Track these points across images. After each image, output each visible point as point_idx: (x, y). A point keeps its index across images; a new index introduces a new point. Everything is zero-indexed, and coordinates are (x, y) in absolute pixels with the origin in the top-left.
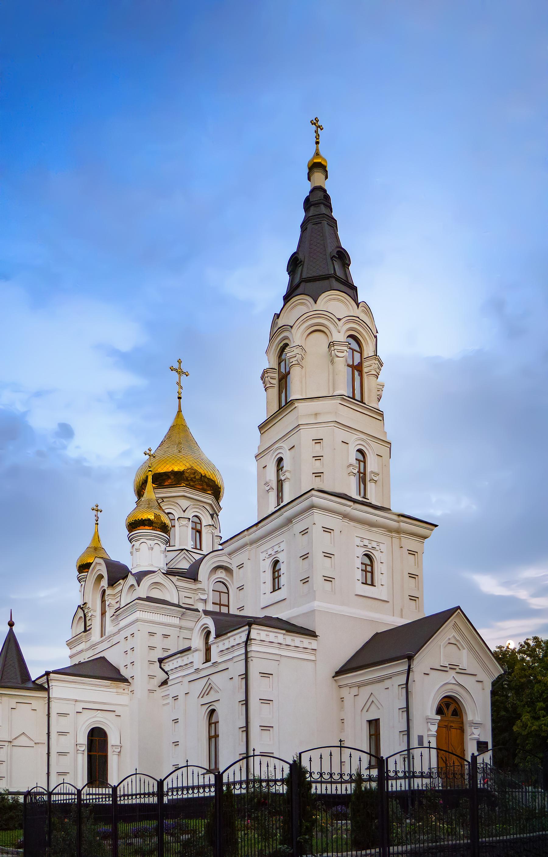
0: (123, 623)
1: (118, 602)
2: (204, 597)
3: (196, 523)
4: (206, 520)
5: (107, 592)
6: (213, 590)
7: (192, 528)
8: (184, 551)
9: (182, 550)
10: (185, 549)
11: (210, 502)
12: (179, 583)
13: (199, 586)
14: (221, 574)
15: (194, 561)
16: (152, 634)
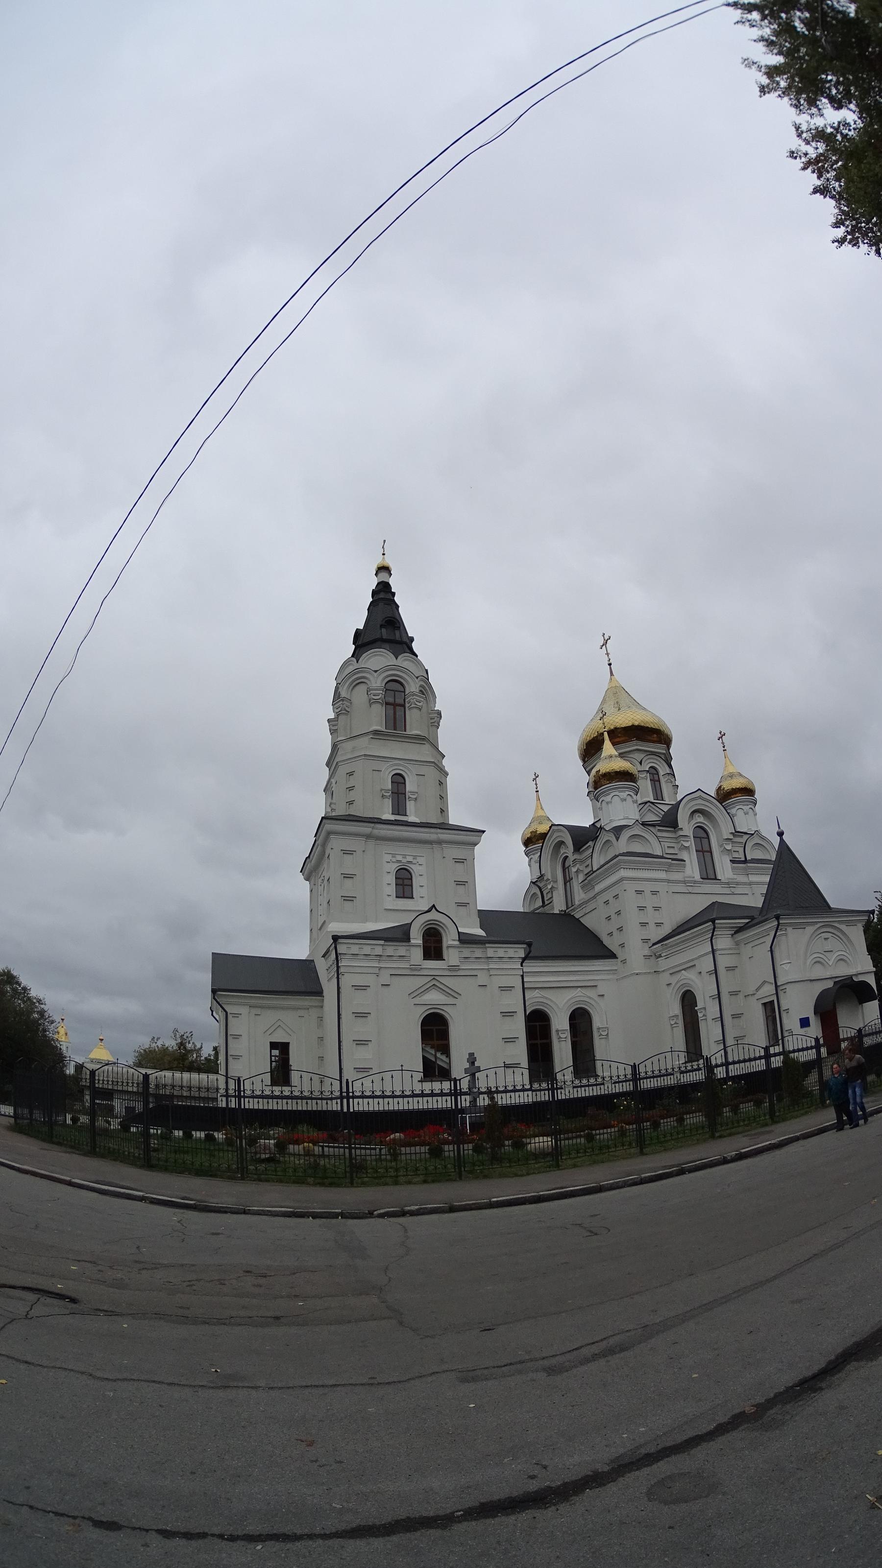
0: (598, 888)
1: (588, 865)
2: (686, 844)
3: (653, 774)
4: (663, 770)
5: (572, 857)
6: (694, 837)
7: (651, 780)
8: (648, 804)
9: (646, 803)
10: (649, 802)
11: (664, 752)
12: (659, 834)
13: (681, 833)
14: (699, 819)
15: (663, 813)
16: (639, 892)
